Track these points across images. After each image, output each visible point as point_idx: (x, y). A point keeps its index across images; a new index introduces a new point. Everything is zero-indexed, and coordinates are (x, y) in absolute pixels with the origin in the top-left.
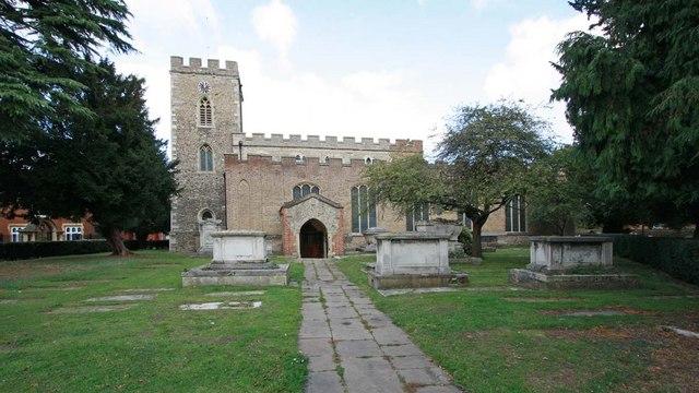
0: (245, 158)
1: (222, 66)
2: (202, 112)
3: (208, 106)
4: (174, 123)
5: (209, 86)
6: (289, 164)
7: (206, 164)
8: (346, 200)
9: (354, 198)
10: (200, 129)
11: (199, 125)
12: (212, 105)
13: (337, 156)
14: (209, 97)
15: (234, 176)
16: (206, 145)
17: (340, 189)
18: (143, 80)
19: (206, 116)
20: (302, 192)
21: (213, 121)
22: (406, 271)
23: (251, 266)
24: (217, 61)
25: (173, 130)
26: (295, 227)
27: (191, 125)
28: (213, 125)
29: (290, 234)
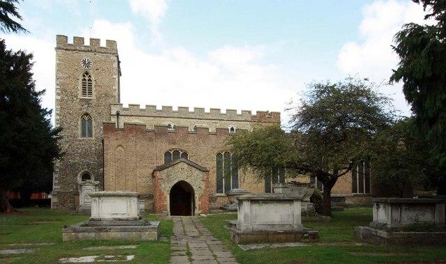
0: (121, 126)
1: (103, 44)
2: (84, 85)
3: (89, 80)
4: (58, 94)
5: (90, 63)
6: (161, 132)
7: (87, 131)
8: (211, 165)
9: (219, 163)
10: (81, 100)
11: (80, 96)
12: (93, 78)
13: (205, 125)
14: (91, 72)
15: (112, 143)
16: (87, 114)
17: (206, 154)
18: (31, 56)
19: (87, 88)
20: (173, 157)
21: (94, 93)
22: (263, 228)
23: (120, 223)
24: (99, 40)
25: (57, 100)
26: (166, 188)
28: (93, 97)
29: (161, 194)
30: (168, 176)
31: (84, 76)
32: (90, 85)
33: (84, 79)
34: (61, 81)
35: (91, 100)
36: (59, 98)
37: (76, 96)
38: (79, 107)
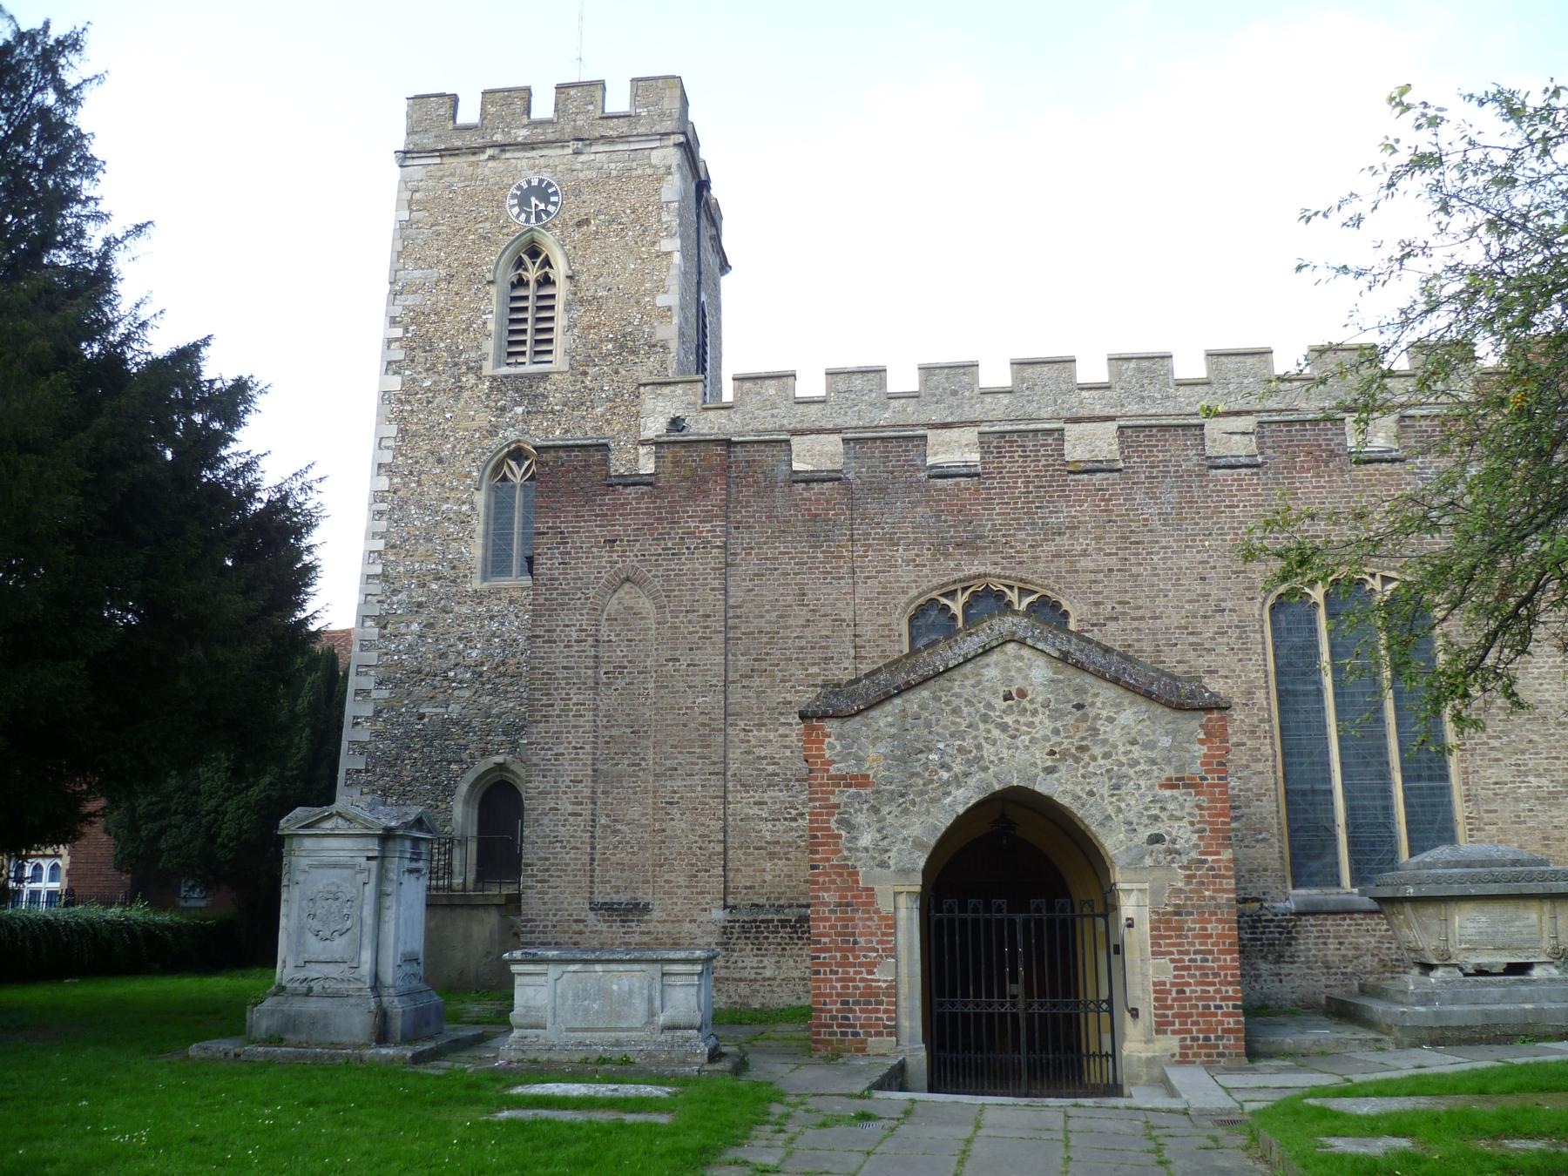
2: (515, 311)
3: (546, 281)
4: (391, 367)
8: (1244, 672)
10: (499, 383)
12: (560, 270)
17: (1202, 603)
18: (72, 43)
21: (561, 340)
24: (601, 84)
25: (385, 396)
26: (891, 857)
27: (463, 366)
28: (558, 361)
29: (857, 899)
30: (906, 755)
31: (520, 264)
32: (545, 305)
33: (521, 283)
34: (410, 300)
35: (545, 376)
36: (395, 383)
37: (476, 370)
38: (484, 419)
